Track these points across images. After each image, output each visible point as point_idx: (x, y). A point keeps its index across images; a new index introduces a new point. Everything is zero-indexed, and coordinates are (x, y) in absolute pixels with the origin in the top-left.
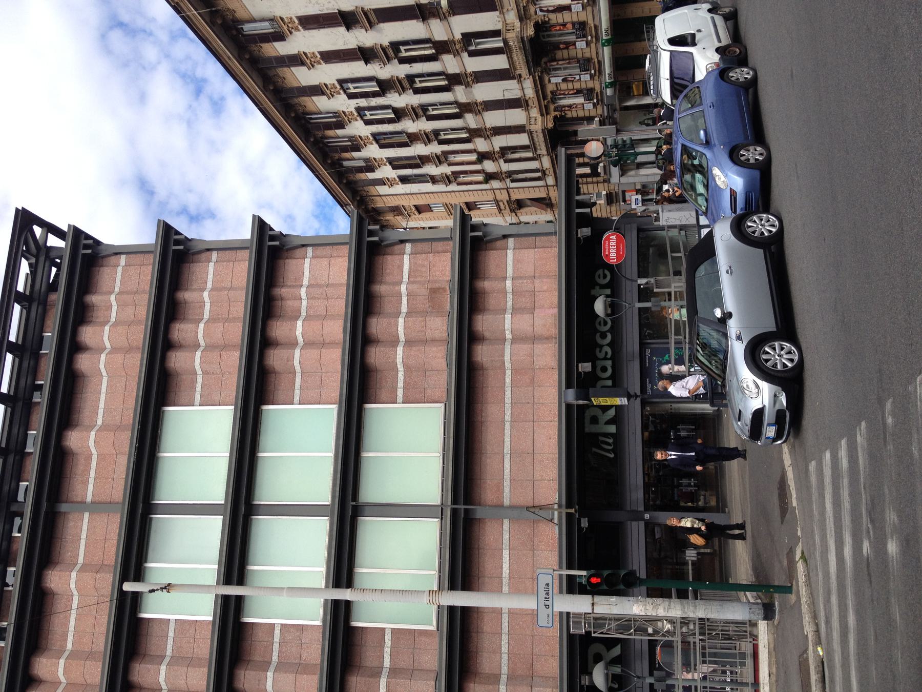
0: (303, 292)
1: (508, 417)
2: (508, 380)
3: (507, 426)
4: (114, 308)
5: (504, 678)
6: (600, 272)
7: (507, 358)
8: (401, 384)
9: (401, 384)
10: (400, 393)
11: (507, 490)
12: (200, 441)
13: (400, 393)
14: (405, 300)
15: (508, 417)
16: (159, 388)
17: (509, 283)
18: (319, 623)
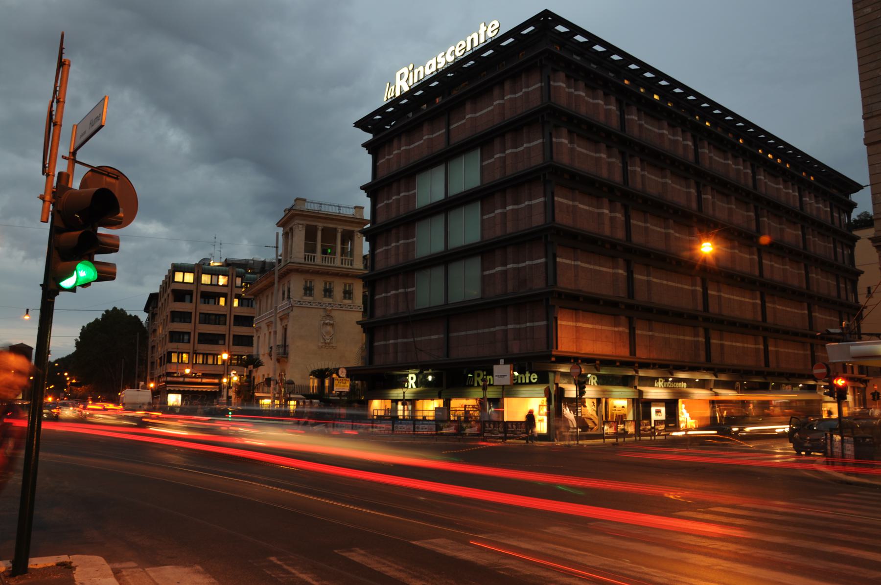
0: (526, 203)
1: (480, 331)
2: (492, 329)
3: (475, 332)
4: (520, 94)
5: (405, 340)
6: (536, 376)
7: (498, 328)
8: (491, 272)
9: (491, 272)
10: (487, 273)
11: (455, 334)
12: (467, 174)
13: (487, 273)
14: (524, 265)
15: (480, 331)
16: (482, 142)
17: (528, 324)
18: (416, 257)
